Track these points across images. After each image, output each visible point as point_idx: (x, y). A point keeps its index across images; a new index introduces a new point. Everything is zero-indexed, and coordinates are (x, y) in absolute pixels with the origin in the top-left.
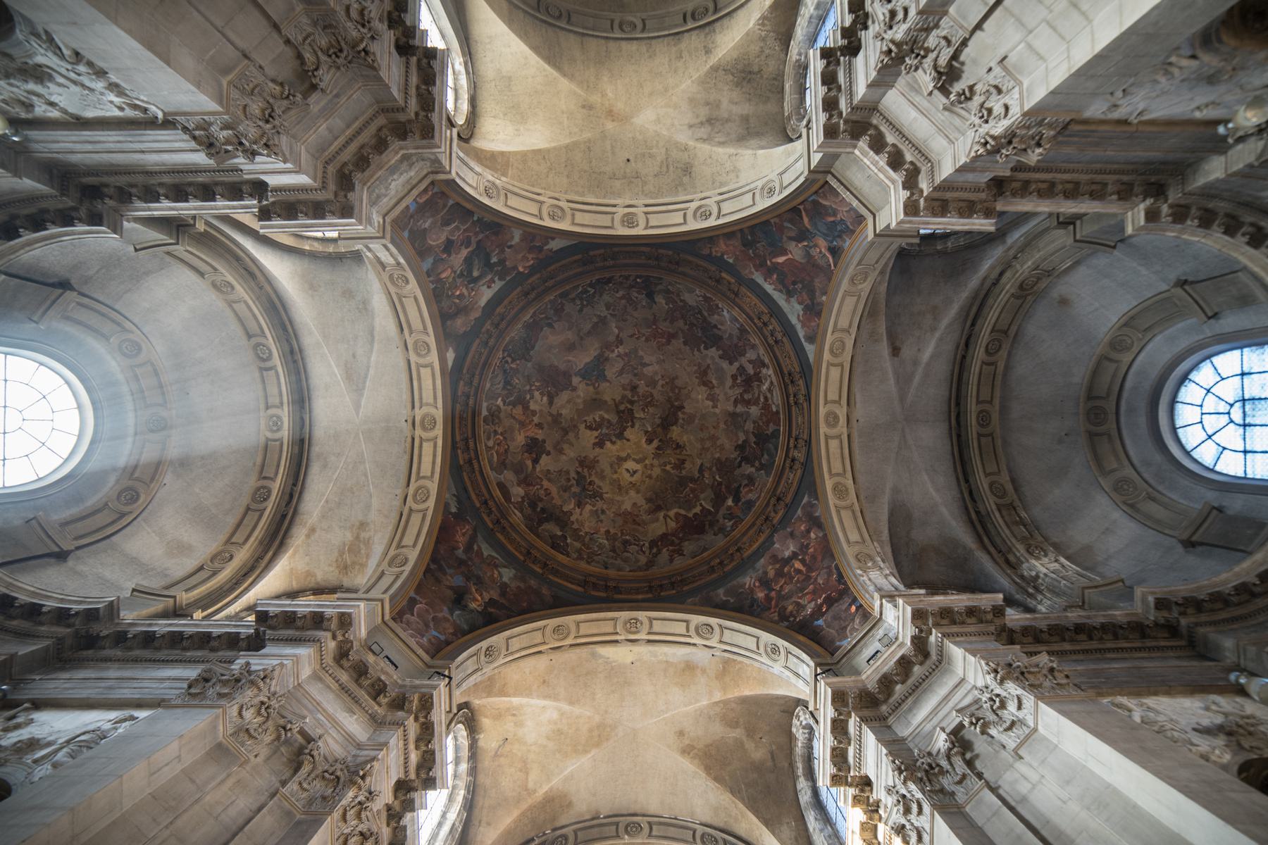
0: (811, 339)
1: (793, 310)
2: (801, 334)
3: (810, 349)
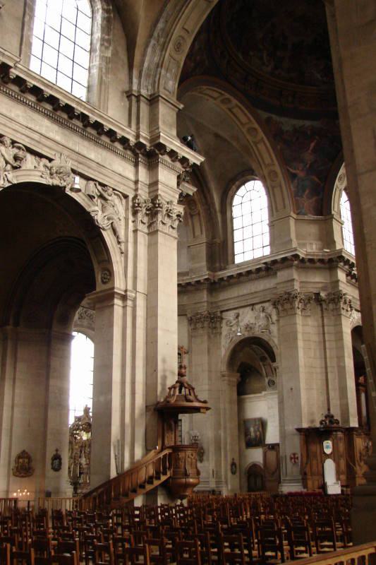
0: (268, 120)
1: (288, 124)
2: (274, 116)
3: (265, 115)
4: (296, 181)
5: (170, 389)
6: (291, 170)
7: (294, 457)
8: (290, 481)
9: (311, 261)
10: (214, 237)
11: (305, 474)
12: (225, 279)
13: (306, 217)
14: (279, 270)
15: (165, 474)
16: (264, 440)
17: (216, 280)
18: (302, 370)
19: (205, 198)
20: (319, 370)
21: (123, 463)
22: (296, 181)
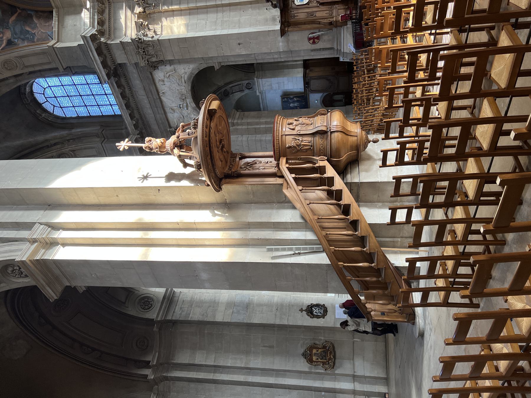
4: (16, 40)
5: (186, 165)
6: (3, 46)
7: (314, 40)
8: (339, 42)
9: (101, 23)
10: (97, 136)
11: (331, 23)
12: (134, 122)
13: (55, 29)
14: (114, 61)
15: (322, 170)
16: (301, 93)
17: (138, 132)
18: (218, 33)
19: (55, 144)
20: (220, 15)
21: (306, 242)
22: (16, 40)
